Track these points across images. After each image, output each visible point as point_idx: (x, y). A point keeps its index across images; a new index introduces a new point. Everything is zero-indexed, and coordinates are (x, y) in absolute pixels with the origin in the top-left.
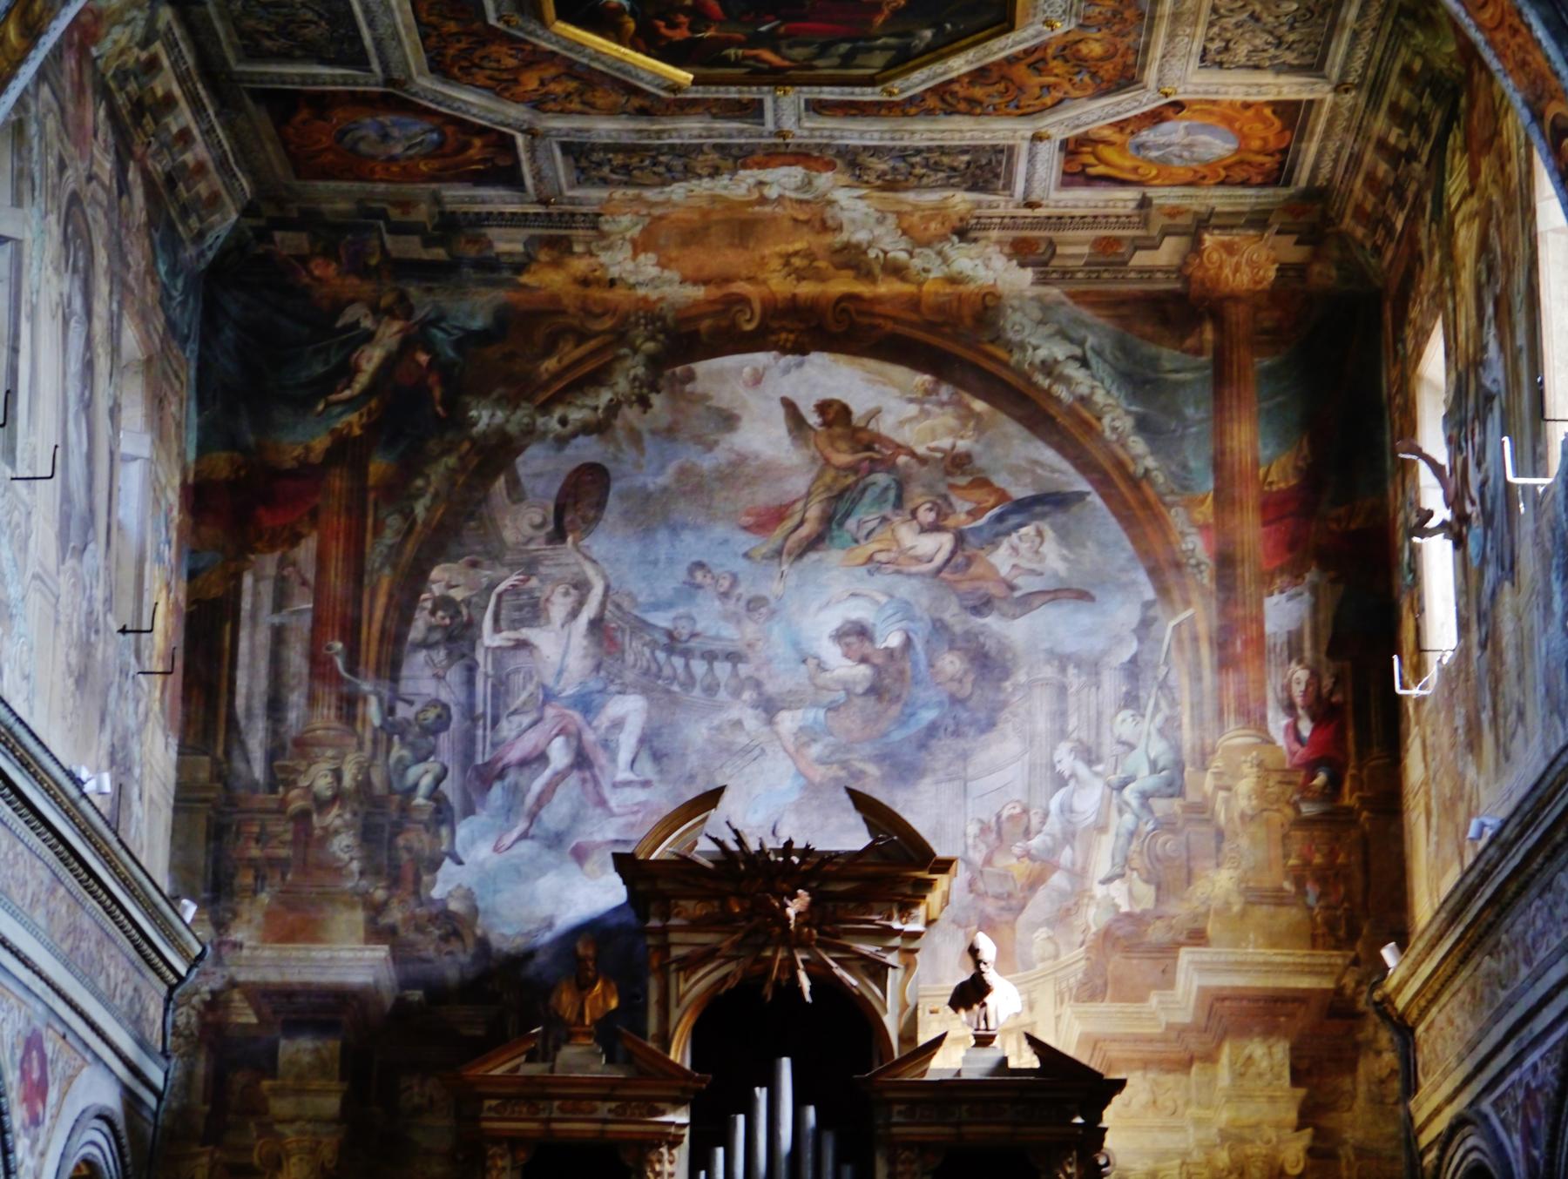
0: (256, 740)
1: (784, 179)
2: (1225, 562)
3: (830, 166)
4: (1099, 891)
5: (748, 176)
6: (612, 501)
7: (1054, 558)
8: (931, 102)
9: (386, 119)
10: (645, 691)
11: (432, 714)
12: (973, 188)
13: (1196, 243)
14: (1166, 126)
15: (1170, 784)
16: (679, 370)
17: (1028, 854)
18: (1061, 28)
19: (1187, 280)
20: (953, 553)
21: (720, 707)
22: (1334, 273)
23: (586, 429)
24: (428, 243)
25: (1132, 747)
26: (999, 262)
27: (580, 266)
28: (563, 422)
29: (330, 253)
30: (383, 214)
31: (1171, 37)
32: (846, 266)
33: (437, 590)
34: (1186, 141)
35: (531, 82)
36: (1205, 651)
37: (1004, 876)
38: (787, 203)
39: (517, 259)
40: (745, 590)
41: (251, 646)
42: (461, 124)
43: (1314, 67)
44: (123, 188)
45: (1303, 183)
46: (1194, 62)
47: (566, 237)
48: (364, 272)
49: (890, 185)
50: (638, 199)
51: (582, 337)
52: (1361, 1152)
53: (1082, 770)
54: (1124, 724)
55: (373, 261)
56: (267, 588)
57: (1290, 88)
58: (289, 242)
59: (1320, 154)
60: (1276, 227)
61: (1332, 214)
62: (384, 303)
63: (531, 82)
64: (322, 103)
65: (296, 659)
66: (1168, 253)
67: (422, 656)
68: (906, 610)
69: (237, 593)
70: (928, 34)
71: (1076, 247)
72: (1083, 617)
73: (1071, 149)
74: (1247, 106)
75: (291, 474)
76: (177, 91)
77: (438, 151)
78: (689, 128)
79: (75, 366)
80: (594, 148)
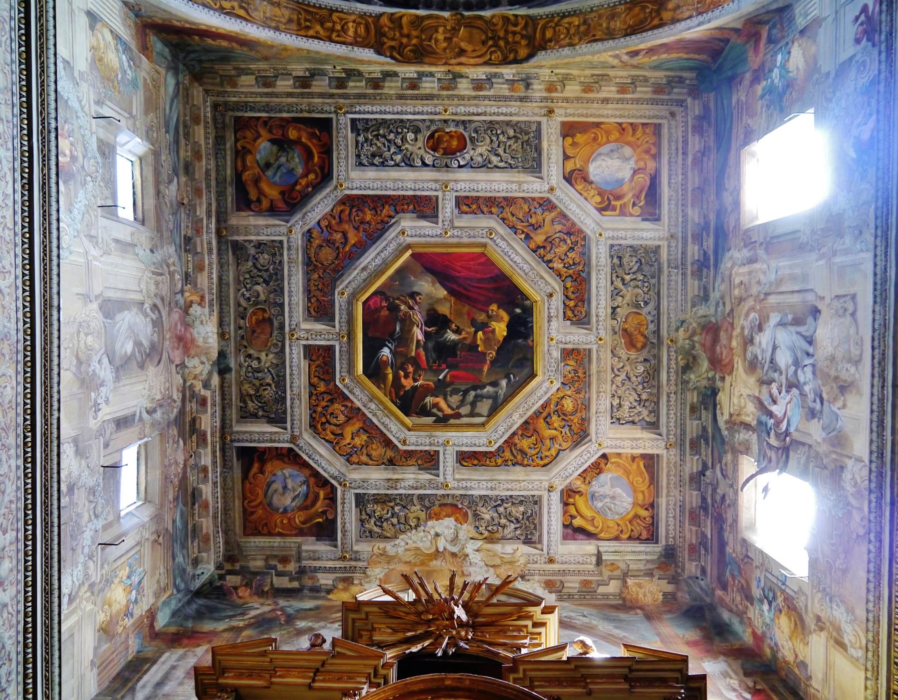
1: (446, 526)
12: (528, 542)
13: (625, 582)
14: (602, 477)
19: (624, 599)
22: (688, 597)
24: (291, 580)
29: (248, 585)
30: (274, 567)
34: (611, 493)
38: (447, 555)
39: (329, 587)
42: (316, 474)
45: (664, 543)
47: (351, 577)
50: (384, 554)
55: (266, 589)
58: (232, 580)
60: (657, 577)
61: (680, 571)
66: (613, 587)
74: (633, 458)
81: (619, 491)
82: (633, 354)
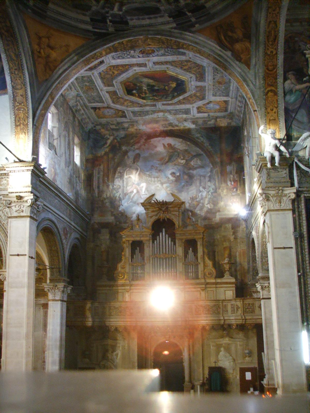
0: (96, 191)
1: (161, 114)
2: (222, 162)
3: (166, 112)
4: (206, 206)
5: (156, 114)
6: (141, 159)
7: (199, 163)
8: (178, 103)
9: (108, 110)
10: (146, 182)
11: (118, 187)
12: (186, 114)
13: (216, 121)
15: (215, 191)
16: (149, 140)
17: (197, 201)
18: (194, 92)
20: (186, 162)
21: (156, 184)
23: (137, 149)
25: (210, 187)
26: (190, 124)
27: (135, 128)
28: (134, 148)
29: (103, 128)
30: (109, 123)
31: (208, 92)
32: (170, 126)
33: (118, 171)
35: (126, 103)
36: (219, 175)
37: (194, 204)
40: (158, 169)
41: (95, 179)
42: (118, 110)
43: (227, 95)
44: (74, 121)
46: (212, 96)
48: (107, 130)
49: (175, 114)
50: (142, 118)
51: (136, 137)
52: (241, 238)
53: (203, 190)
54: (209, 184)
56: (97, 172)
57: (225, 99)
58: (98, 128)
59: (231, 108)
62: (111, 134)
63: (126, 103)
64: (99, 108)
65: (101, 181)
66: (212, 122)
67: (117, 179)
68: (179, 170)
69: (93, 173)
70: (176, 94)
71: (200, 122)
72: (203, 170)
73: (198, 108)
74: (220, 101)
75: (99, 157)
76: (81, 108)
77: (115, 114)
78: (147, 108)
79: (67, 143)
80: (135, 112)
81: (215, 106)
82: (221, 85)
